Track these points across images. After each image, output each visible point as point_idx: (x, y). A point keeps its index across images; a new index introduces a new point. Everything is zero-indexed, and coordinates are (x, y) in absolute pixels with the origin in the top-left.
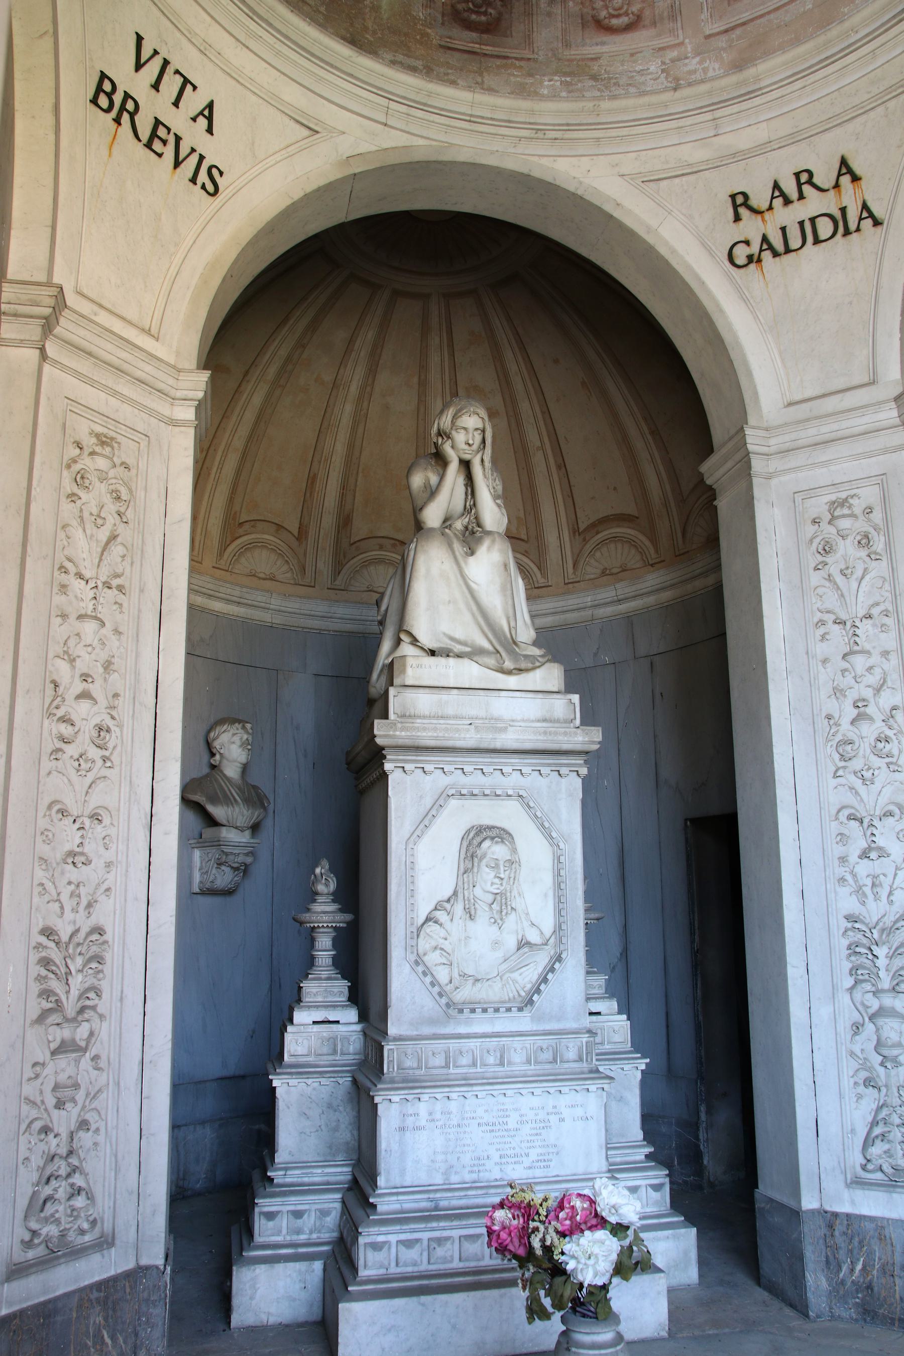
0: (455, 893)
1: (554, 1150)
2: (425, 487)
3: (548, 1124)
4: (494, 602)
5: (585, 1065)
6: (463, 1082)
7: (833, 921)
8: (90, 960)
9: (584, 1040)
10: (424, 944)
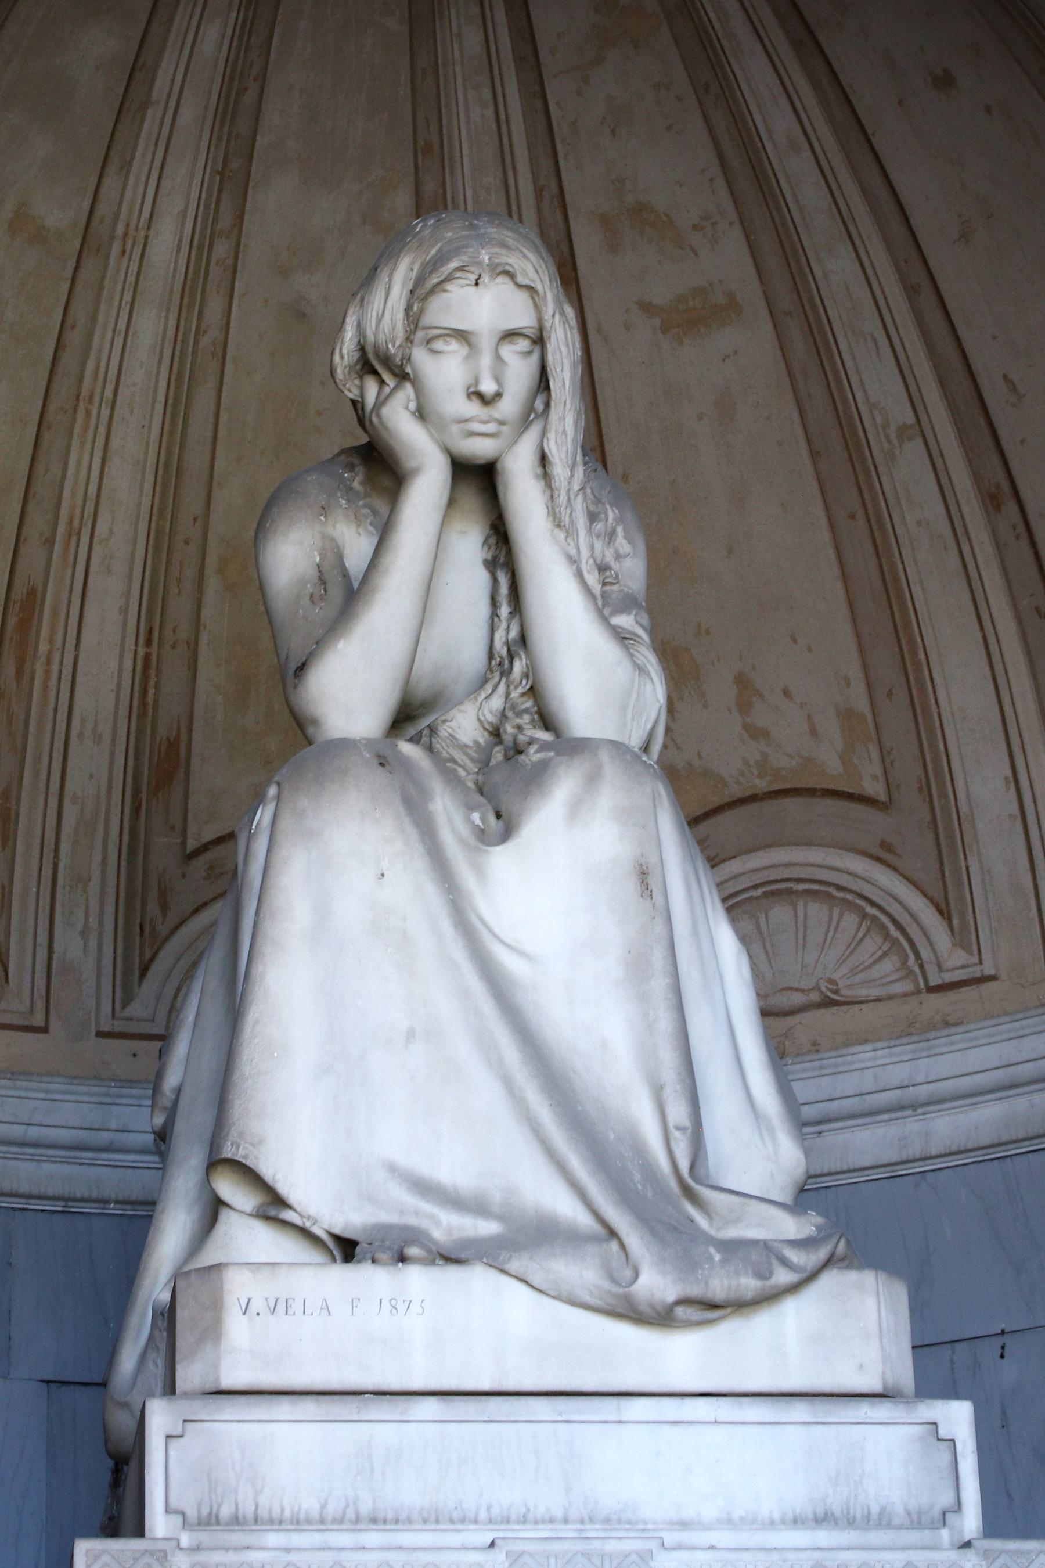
2: (322, 580)
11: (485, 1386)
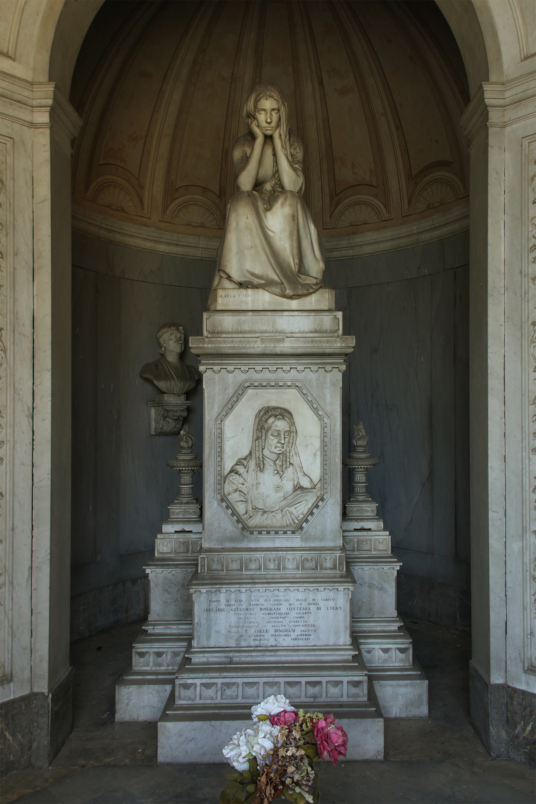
0: (250, 454)
1: (313, 628)
2: (242, 159)
3: (310, 611)
4: (284, 245)
5: (338, 572)
6: (250, 581)
7: (526, 481)
9: (338, 555)
10: (228, 488)
11: (261, 309)
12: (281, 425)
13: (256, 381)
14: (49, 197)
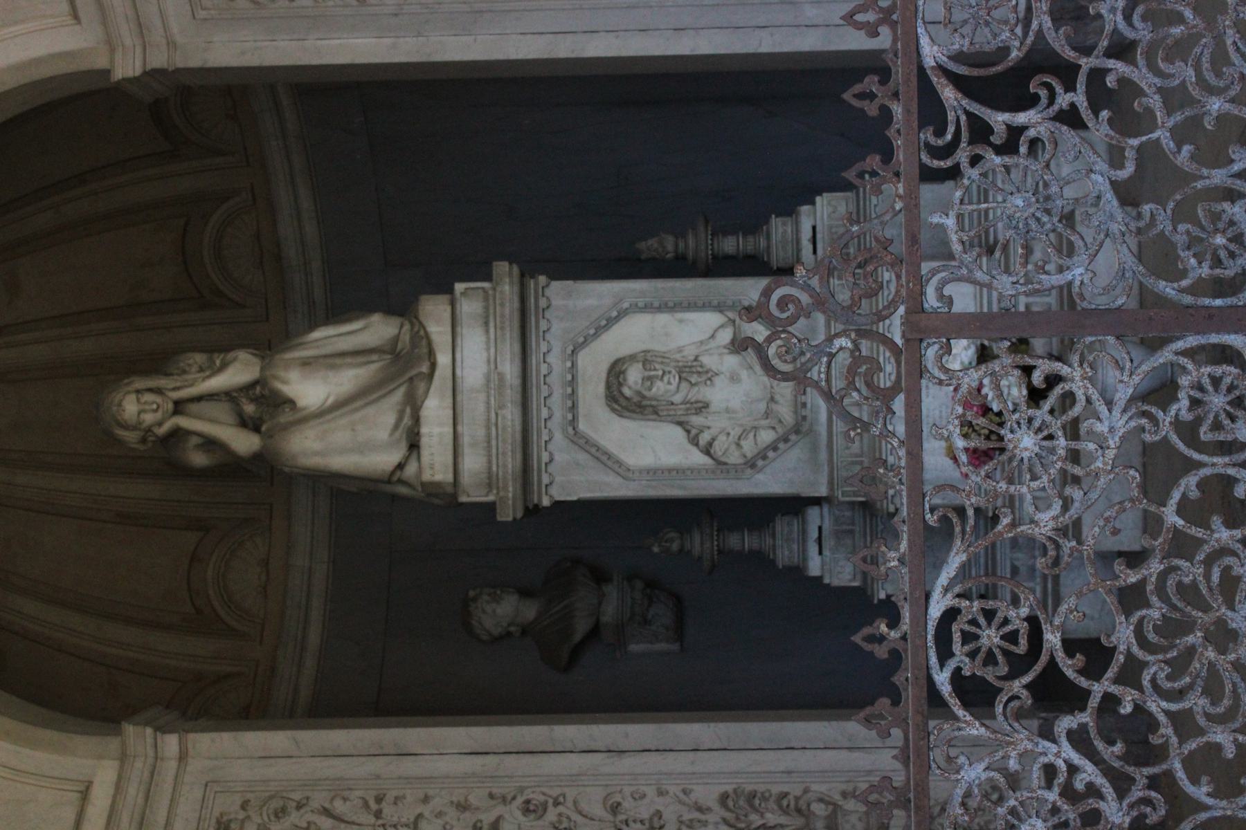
0: (680, 424)
4: (347, 379)
8: (752, 806)
10: (734, 458)
11: (451, 412)
12: (634, 375)
13: (564, 417)
14: (289, 733)
